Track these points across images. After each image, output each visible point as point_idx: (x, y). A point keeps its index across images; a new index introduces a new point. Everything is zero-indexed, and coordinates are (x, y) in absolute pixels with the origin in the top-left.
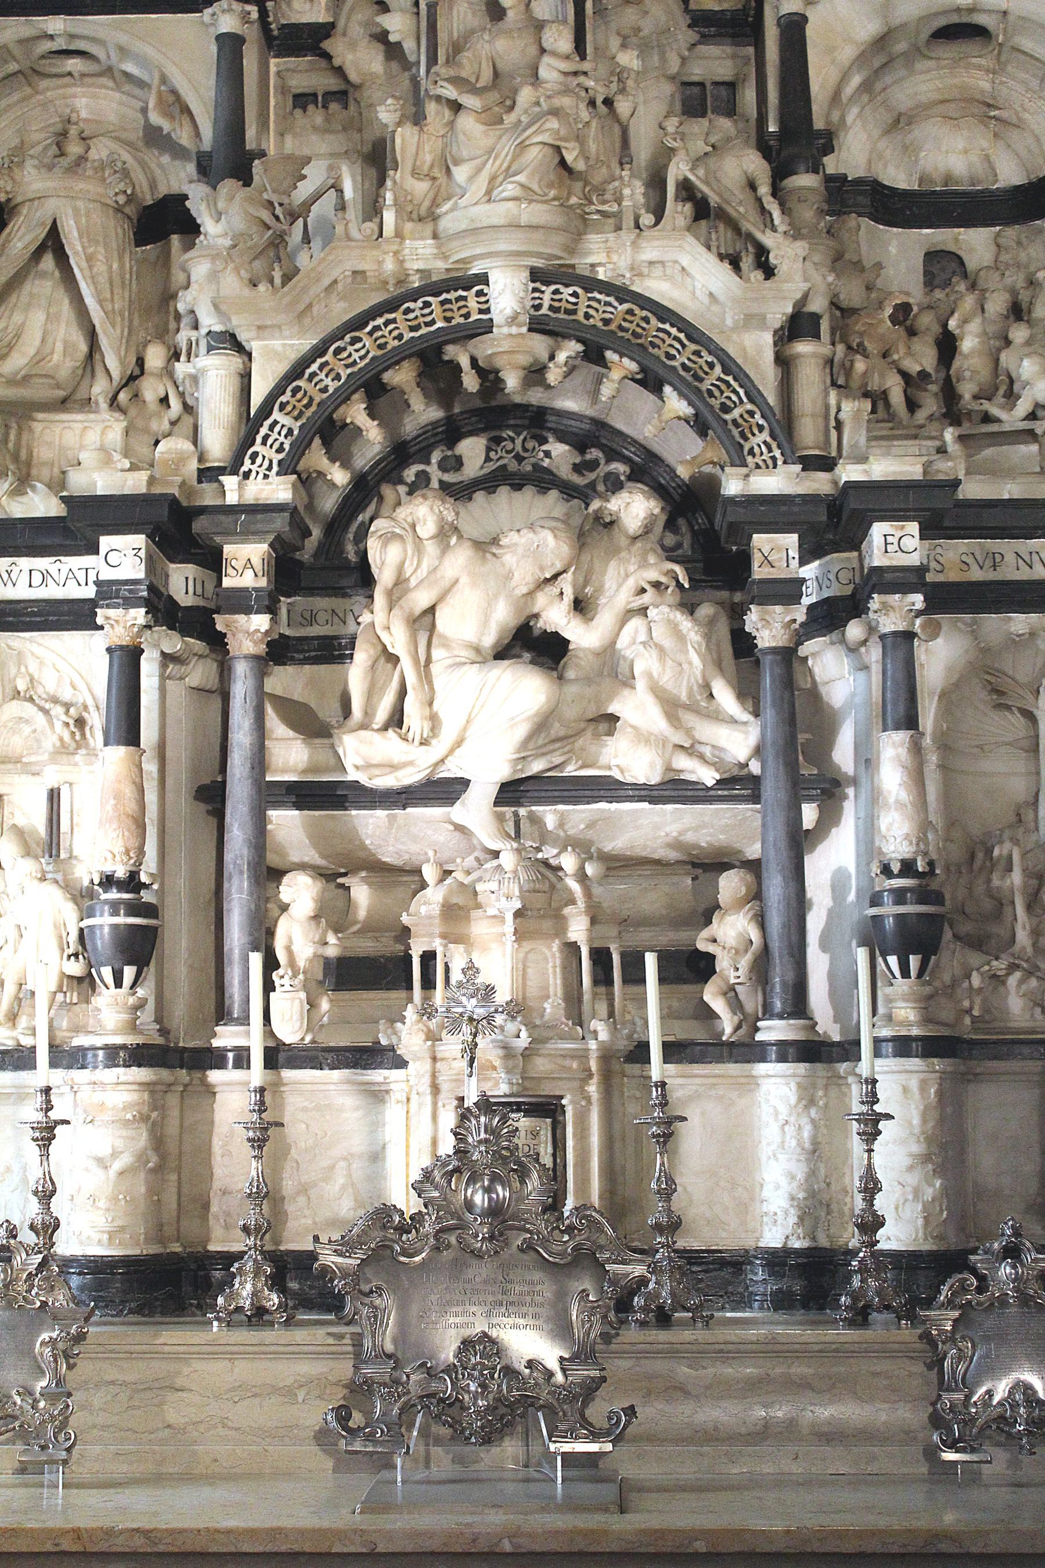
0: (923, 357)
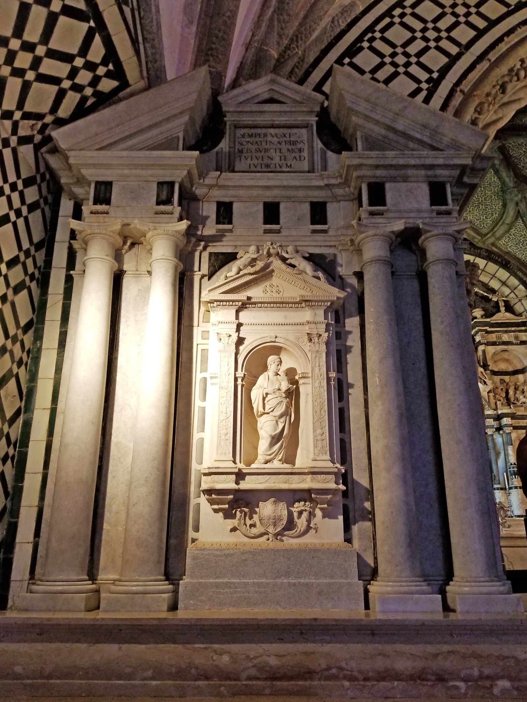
0: (504, 395)
